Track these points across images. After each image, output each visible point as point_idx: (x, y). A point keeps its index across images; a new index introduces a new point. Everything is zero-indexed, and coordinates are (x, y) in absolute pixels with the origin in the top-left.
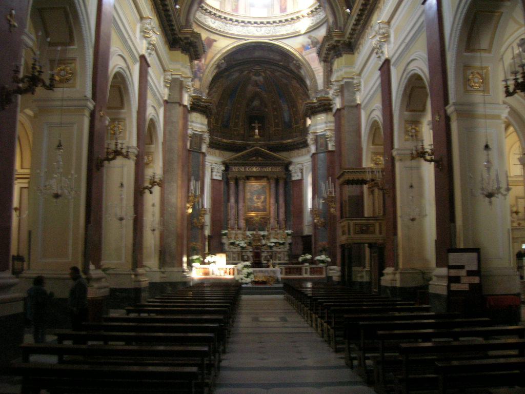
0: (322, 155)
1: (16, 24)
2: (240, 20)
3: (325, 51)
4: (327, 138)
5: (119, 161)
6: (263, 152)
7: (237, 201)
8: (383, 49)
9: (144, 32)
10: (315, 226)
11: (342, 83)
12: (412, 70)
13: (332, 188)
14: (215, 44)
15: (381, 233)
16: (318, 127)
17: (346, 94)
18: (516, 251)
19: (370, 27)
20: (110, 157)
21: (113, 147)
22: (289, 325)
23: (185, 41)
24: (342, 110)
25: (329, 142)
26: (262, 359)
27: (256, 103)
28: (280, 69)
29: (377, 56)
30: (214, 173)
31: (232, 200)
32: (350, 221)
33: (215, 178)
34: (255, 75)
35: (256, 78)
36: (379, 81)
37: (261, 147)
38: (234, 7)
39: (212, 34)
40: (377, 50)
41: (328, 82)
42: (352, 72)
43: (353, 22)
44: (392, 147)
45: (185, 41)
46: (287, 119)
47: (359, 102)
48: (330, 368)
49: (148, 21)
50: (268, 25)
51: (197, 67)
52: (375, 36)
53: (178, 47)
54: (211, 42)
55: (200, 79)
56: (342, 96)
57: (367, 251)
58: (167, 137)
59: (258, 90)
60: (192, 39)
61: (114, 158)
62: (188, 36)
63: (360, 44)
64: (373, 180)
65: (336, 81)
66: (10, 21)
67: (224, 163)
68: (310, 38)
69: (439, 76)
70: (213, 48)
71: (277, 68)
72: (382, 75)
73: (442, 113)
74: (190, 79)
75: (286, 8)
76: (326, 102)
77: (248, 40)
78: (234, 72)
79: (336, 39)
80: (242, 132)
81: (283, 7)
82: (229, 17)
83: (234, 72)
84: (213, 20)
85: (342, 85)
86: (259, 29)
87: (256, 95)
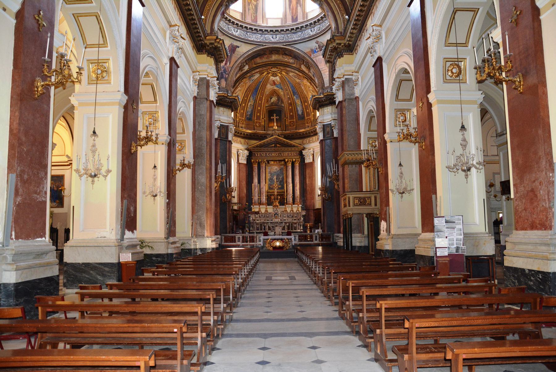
0: (328, 141)
1: (45, 25)
2: (259, 28)
3: (328, 53)
4: (333, 127)
5: (150, 145)
6: (281, 140)
7: (259, 182)
8: (376, 48)
9: (174, 39)
10: (324, 201)
11: (343, 79)
12: (400, 65)
13: (335, 168)
14: (237, 49)
15: (376, 205)
16: (325, 118)
17: (347, 88)
18: (494, 219)
19: (365, 31)
20: (142, 143)
21: (143, 134)
22: (295, 282)
23: (210, 46)
24: (344, 103)
25: (334, 130)
26: (267, 312)
27: (274, 99)
28: (293, 70)
29: (371, 54)
30: (240, 158)
31: (256, 180)
32: (350, 195)
33: (240, 162)
34: (273, 76)
35: (274, 78)
36: (373, 76)
37: (278, 136)
38: (253, 18)
39: (235, 41)
40: (371, 50)
41: (332, 79)
42: (350, 71)
43: (351, 26)
44: (384, 132)
45: (210, 46)
46: (300, 113)
47: (357, 95)
48: (327, 319)
49: (177, 28)
50: (282, 32)
51: (223, 69)
52: (369, 37)
53: (204, 51)
54: (233, 49)
55: (226, 80)
56: (344, 90)
57: (366, 219)
58: (197, 127)
59: (275, 88)
60: (216, 44)
61: (146, 143)
62: (213, 42)
63: (357, 46)
64: (368, 160)
65: (338, 78)
66: (38, 20)
67: (247, 149)
68: (317, 43)
69: (422, 69)
70: (236, 52)
71: (291, 69)
72: (375, 71)
73: (425, 100)
74: (216, 79)
75: (297, 18)
76: (330, 97)
77: (265, 46)
78: (255, 73)
79: (338, 41)
80: (263, 124)
81: (295, 17)
82: (249, 26)
83: (255, 73)
84: (236, 30)
85: (343, 81)
86: (274, 36)
87: (274, 93)
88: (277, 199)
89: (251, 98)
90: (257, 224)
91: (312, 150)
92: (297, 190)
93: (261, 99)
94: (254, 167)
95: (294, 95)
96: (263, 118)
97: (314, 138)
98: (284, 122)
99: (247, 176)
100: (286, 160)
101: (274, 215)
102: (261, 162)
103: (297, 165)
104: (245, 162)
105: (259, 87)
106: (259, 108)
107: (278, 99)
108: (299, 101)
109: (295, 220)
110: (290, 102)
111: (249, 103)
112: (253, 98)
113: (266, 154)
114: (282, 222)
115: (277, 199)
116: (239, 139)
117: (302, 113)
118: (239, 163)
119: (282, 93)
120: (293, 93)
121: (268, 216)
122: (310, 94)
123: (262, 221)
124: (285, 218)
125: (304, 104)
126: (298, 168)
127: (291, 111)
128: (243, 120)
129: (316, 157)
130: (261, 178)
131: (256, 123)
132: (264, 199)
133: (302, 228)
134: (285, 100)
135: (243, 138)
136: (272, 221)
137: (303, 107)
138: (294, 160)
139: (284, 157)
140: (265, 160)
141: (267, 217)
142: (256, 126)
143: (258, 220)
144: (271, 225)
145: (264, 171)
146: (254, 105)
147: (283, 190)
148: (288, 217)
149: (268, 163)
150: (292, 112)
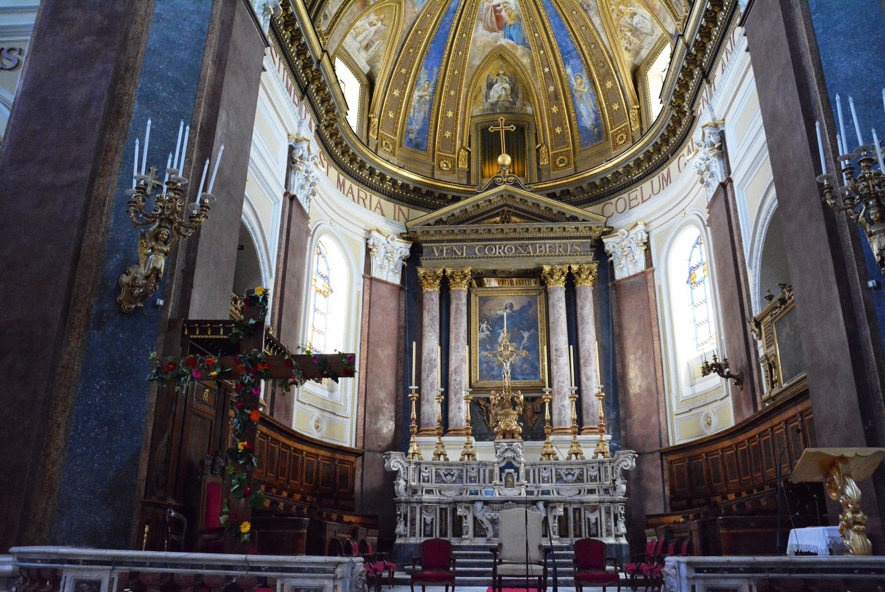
6: (524, 201)
30: (376, 261)
33: (376, 273)
46: (588, 121)
59: (503, 41)
67: (408, 236)
80: (463, 165)
88: (514, 404)
89: (423, 76)
90: (425, 507)
91: (641, 227)
92: (588, 379)
93: (456, 83)
94: (426, 296)
95: (566, 61)
96: (462, 147)
98: (534, 159)
99: (399, 328)
100: (547, 268)
101: (502, 470)
102: (452, 276)
103: (586, 288)
104: (396, 280)
105: (447, 33)
106: (450, 114)
107: (513, 90)
108: (585, 80)
109: (591, 491)
110: (552, 89)
111: (416, 94)
113: (473, 248)
114: (534, 503)
115: (514, 404)
116: (375, 199)
117: (597, 119)
118: (371, 279)
119: (525, 61)
120: (563, 54)
121: (473, 474)
122: (624, 43)
123: (451, 495)
124: (545, 486)
126: (590, 296)
127: (556, 120)
128: (394, 144)
129: (658, 257)
130: (452, 336)
132: (461, 412)
133: (623, 529)
134: (538, 86)
135: (391, 197)
136: (488, 497)
137: (598, 99)
138: (575, 268)
139: (537, 260)
140: (467, 270)
141: (471, 480)
142: (440, 168)
143: (429, 492)
144: (484, 515)
145: (464, 309)
146: (431, 101)
147: (535, 382)
148: (559, 478)
149: (481, 284)
150: (562, 125)
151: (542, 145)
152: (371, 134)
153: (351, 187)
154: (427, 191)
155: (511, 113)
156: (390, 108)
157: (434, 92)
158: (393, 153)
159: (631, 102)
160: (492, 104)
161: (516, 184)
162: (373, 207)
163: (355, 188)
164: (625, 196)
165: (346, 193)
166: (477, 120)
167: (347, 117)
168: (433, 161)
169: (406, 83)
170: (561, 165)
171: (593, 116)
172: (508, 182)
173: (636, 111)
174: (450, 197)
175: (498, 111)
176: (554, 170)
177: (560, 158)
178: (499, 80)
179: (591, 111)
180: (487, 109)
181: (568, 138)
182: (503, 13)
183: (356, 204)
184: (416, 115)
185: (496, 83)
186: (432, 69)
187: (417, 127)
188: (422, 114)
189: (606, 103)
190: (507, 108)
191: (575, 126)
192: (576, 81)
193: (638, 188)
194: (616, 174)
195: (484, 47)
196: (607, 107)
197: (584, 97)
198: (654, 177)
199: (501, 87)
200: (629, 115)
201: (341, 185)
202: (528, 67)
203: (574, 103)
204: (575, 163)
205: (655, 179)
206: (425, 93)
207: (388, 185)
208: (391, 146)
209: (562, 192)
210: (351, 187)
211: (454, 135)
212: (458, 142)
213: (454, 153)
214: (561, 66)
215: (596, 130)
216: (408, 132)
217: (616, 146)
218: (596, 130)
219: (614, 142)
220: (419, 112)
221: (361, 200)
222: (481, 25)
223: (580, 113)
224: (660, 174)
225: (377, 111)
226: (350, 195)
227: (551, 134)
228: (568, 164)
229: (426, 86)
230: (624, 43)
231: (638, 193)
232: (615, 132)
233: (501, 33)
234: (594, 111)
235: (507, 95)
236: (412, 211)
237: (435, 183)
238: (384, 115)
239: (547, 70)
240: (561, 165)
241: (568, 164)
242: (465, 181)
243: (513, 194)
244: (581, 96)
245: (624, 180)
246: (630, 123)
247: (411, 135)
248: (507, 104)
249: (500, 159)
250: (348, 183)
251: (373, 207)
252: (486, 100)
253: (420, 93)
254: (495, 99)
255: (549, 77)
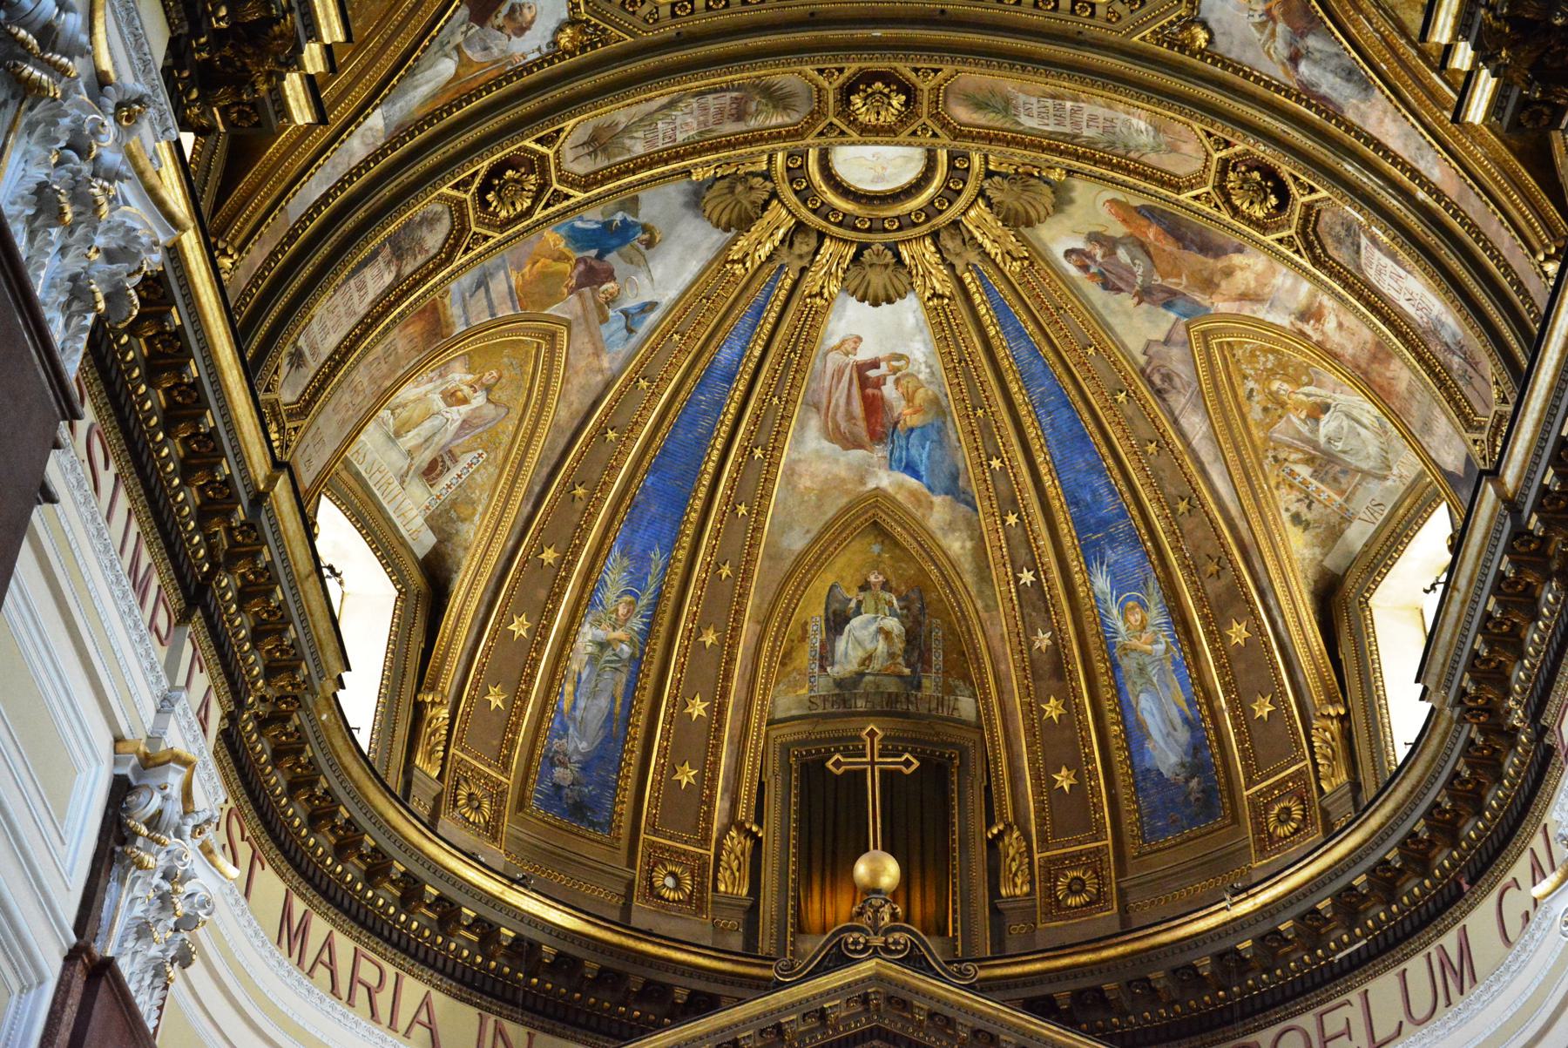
59: (885, 479)
80: (732, 884)
89: (615, 576)
95: (1091, 553)
96: (733, 821)
97: (1383, 988)
105: (703, 443)
106: (698, 708)
108: (1156, 614)
110: (1043, 640)
111: (587, 634)
112: (634, 589)
116: (414, 990)
117: (1196, 747)
119: (957, 545)
120: (1081, 525)
122: (1287, 500)
125: (1217, 636)
128: (498, 797)
131: (658, 857)
137: (1201, 681)
142: (653, 892)
146: (636, 661)
150: (1077, 765)
151: (1009, 827)
152: (419, 760)
153: (328, 943)
154: (603, 971)
155: (905, 715)
156: (492, 676)
157: (648, 633)
158: (492, 830)
159: (1315, 695)
160: (840, 683)
161: (914, 960)
162: (404, 1020)
163: (345, 946)
164: (1307, 1021)
165: (308, 963)
166: (787, 733)
167: (341, 694)
168: (631, 864)
169: (555, 597)
170: (1072, 901)
171: (1183, 735)
172: (886, 949)
173: (1335, 726)
174: (681, 995)
175: (861, 705)
176: (1049, 916)
177: (1072, 874)
178: (869, 603)
179: (1178, 721)
180: (825, 699)
181: (1098, 808)
182: (889, 391)
183: (341, 1007)
184: (582, 703)
185: (858, 612)
186: (643, 559)
187: (583, 746)
188: (603, 702)
189: (1226, 692)
190: (892, 699)
191: (1121, 770)
192: (1125, 620)
193: (1354, 996)
194: (1270, 941)
195: (822, 495)
196: (1232, 709)
197: (1153, 672)
198: (1407, 957)
199: (873, 628)
200: (1308, 737)
201: (292, 935)
202: (967, 565)
203: (1118, 689)
204: (1122, 894)
205: (1416, 967)
206: (619, 634)
207: (462, 943)
208: (486, 805)
209: (1078, 996)
210: (328, 943)
211: (707, 779)
212: (720, 804)
213: (705, 841)
214: (1075, 566)
215: (1194, 783)
216: (551, 761)
217: (1265, 842)
218: (1194, 783)
219: (1260, 827)
220: (594, 695)
221: (361, 992)
222: (814, 423)
223: (1141, 725)
224: (1432, 949)
225: (449, 683)
226: (322, 973)
227: (1038, 793)
228: (1098, 900)
229: (622, 610)
230: (1287, 500)
231: (1355, 1013)
232: (1261, 793)
233: (880, 452)
234: (1186, 720)
235: (892, 655)
236: (541, 1038)
237: (631, 943)
238: (471, 698)
239: (1027, 577)
240: (1072, 901)
241: (1098, 900)
242: (736, 942)
243: (904, 995)
244: (1142, 670)
245: (1298, 962)
246: (1315, 765)
247: (558, 772)
248: (892, 686)
249: (862, 869)
250: (320, 927)
251: (404, 1020)
252: (823, 668)
253: (601, 634)
254: (852, 666)
255: (1034, 602)
